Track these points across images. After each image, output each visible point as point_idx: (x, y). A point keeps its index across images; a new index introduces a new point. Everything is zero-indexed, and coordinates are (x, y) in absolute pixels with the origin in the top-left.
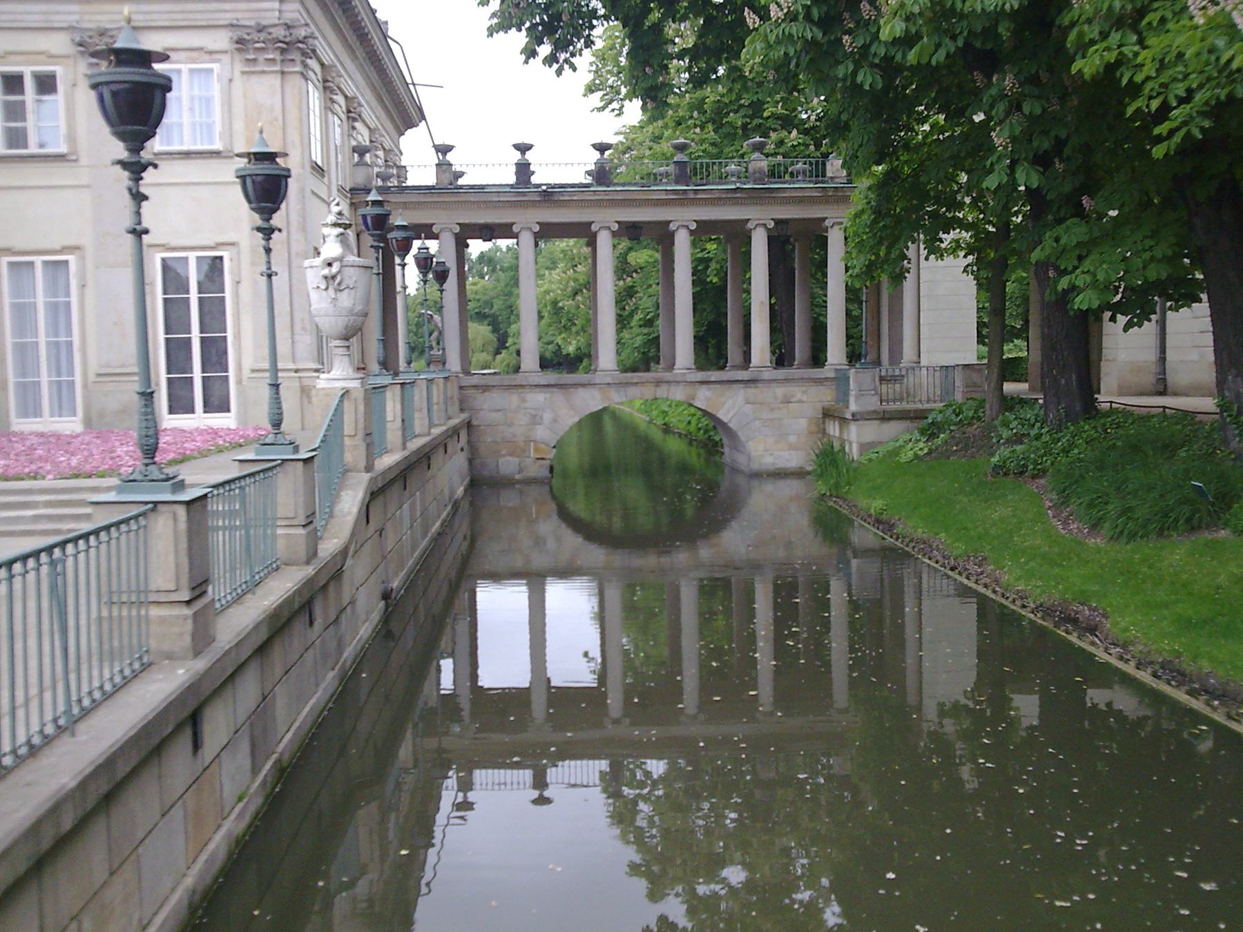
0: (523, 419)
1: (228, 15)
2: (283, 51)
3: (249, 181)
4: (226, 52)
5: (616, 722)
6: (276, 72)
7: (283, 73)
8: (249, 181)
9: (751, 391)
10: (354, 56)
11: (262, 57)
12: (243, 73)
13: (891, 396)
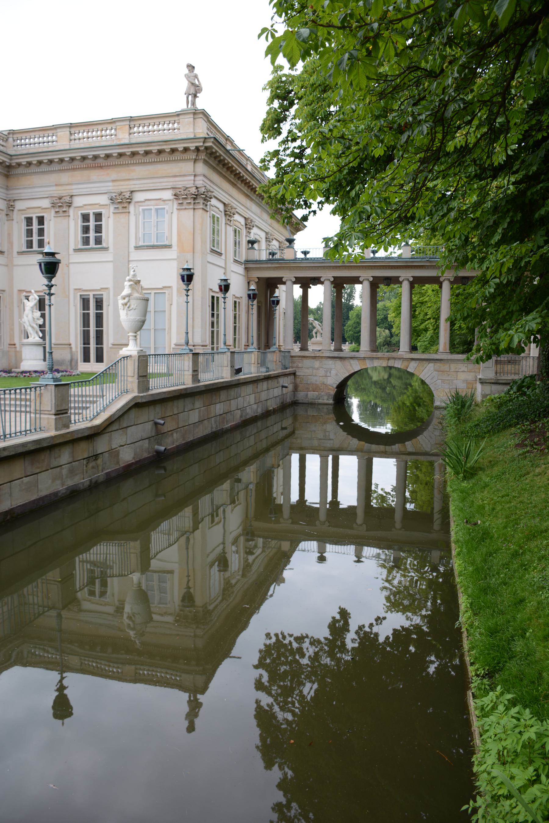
0: (322, 372)
1: (171, 184)
2: (195, 199)
3: (43, 265)
4: (170, 200)
5: (323, 523)
7: (194, 209)
8: (43, 265)
9: (438, 365)
10: (252, 200)
11: (185, 202)
12: (178, 209)
13: (513, 371)
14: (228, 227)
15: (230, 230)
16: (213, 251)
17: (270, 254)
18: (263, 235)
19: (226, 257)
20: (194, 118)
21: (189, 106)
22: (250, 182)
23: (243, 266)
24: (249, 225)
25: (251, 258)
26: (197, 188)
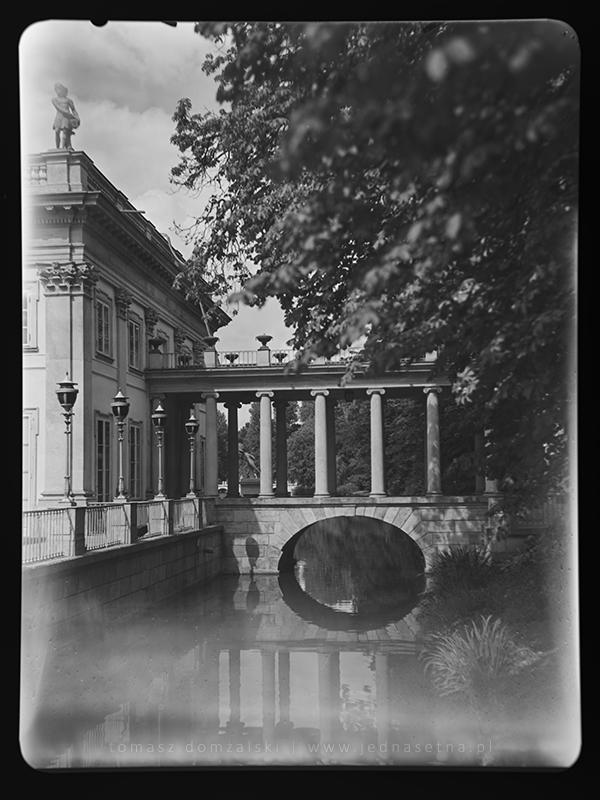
2: (71, 282)
6: (67, 295)
10: (153, 283)
12: (46, 296)
14: (121, 321)
15: (124, 326)
16: (99, 356)
17: (181, 359)
18: (170, 332)
19: (118, 365)
20: (68, 165)
21: (61, 146)
22: (151, 257)
23: (143, 378)
24: (151, 319)
25: (152, 367)
26: (75, 265)
